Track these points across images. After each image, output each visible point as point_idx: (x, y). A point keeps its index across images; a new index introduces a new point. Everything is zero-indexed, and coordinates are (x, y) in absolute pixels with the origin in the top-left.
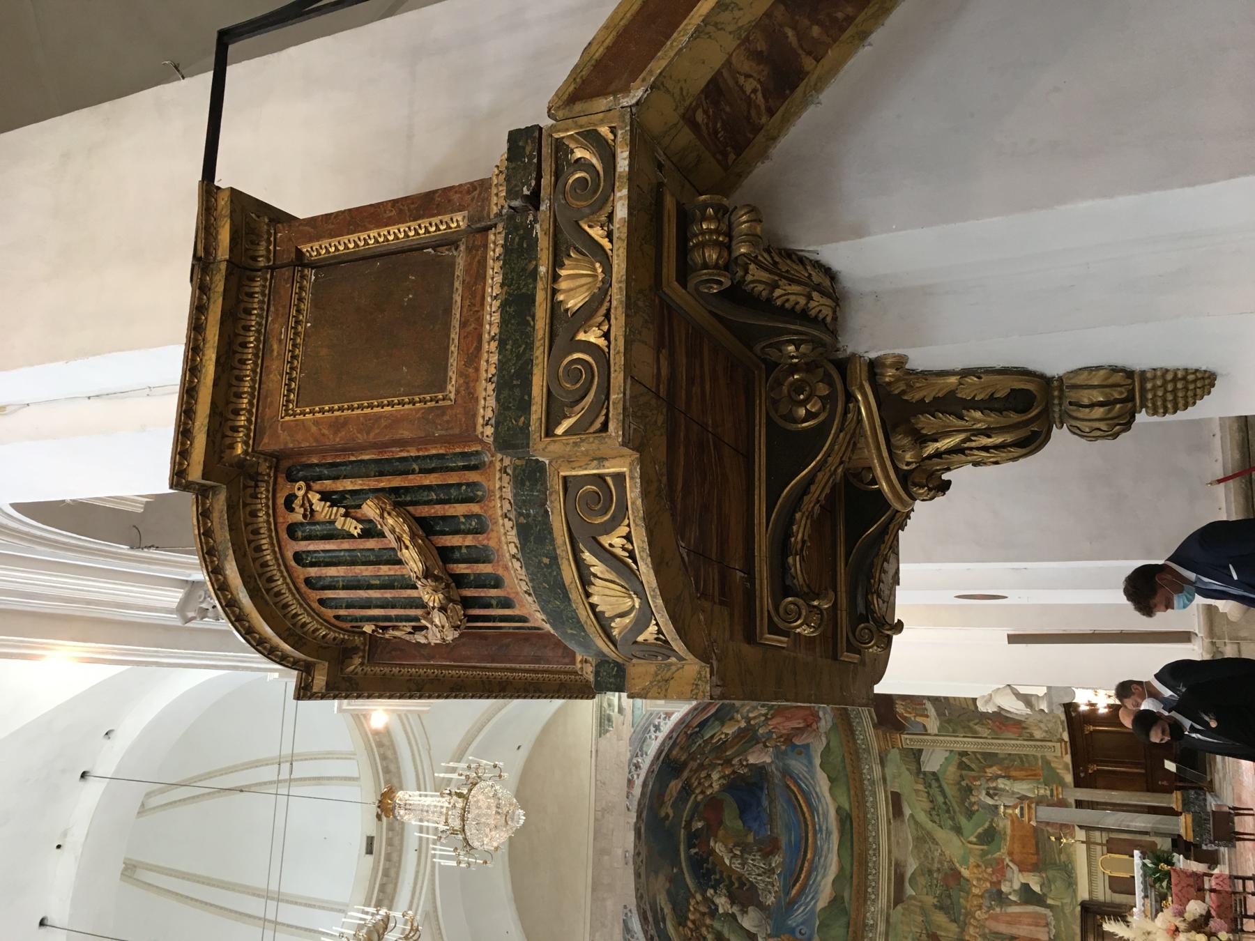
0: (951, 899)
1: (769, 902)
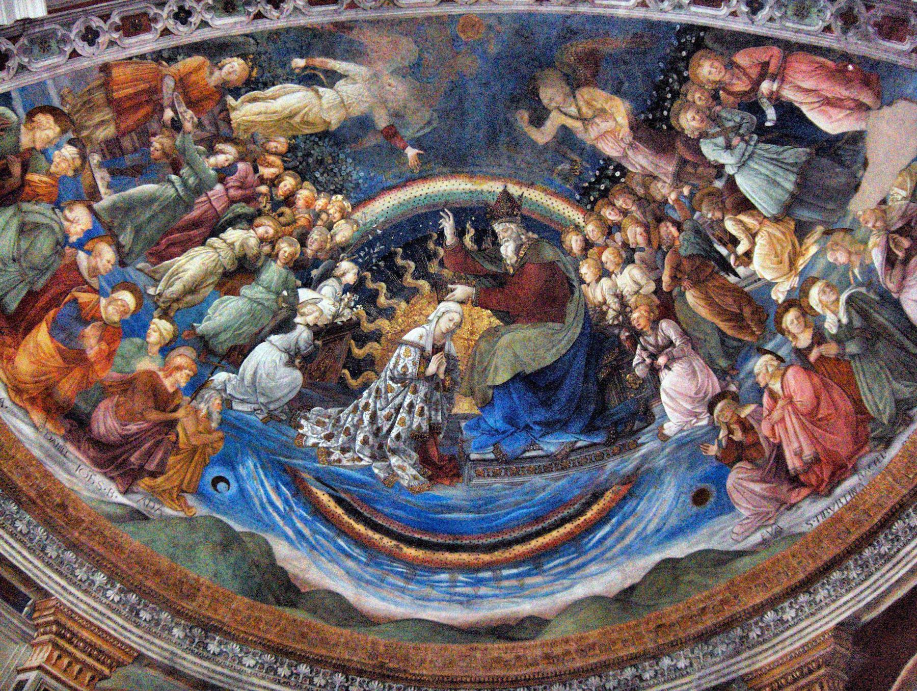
1: (306, 428)
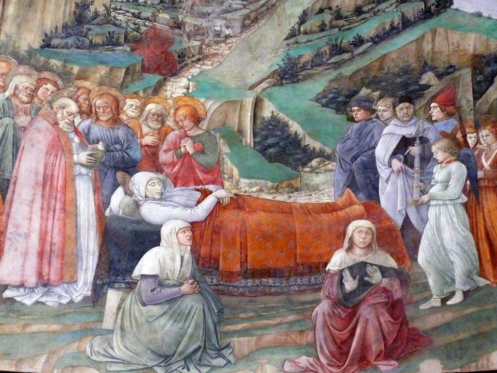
0: (104, 44)
